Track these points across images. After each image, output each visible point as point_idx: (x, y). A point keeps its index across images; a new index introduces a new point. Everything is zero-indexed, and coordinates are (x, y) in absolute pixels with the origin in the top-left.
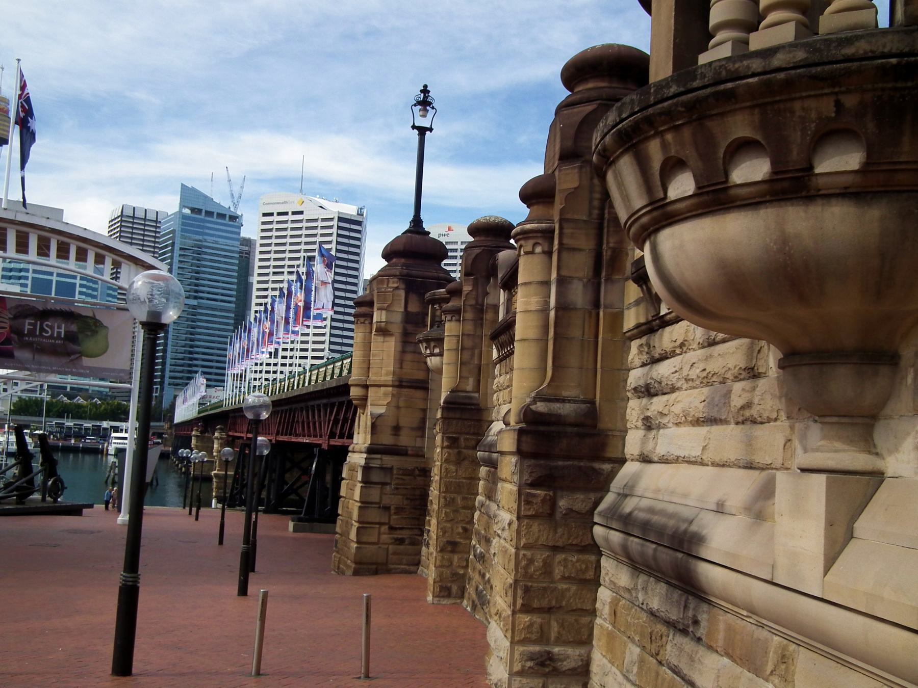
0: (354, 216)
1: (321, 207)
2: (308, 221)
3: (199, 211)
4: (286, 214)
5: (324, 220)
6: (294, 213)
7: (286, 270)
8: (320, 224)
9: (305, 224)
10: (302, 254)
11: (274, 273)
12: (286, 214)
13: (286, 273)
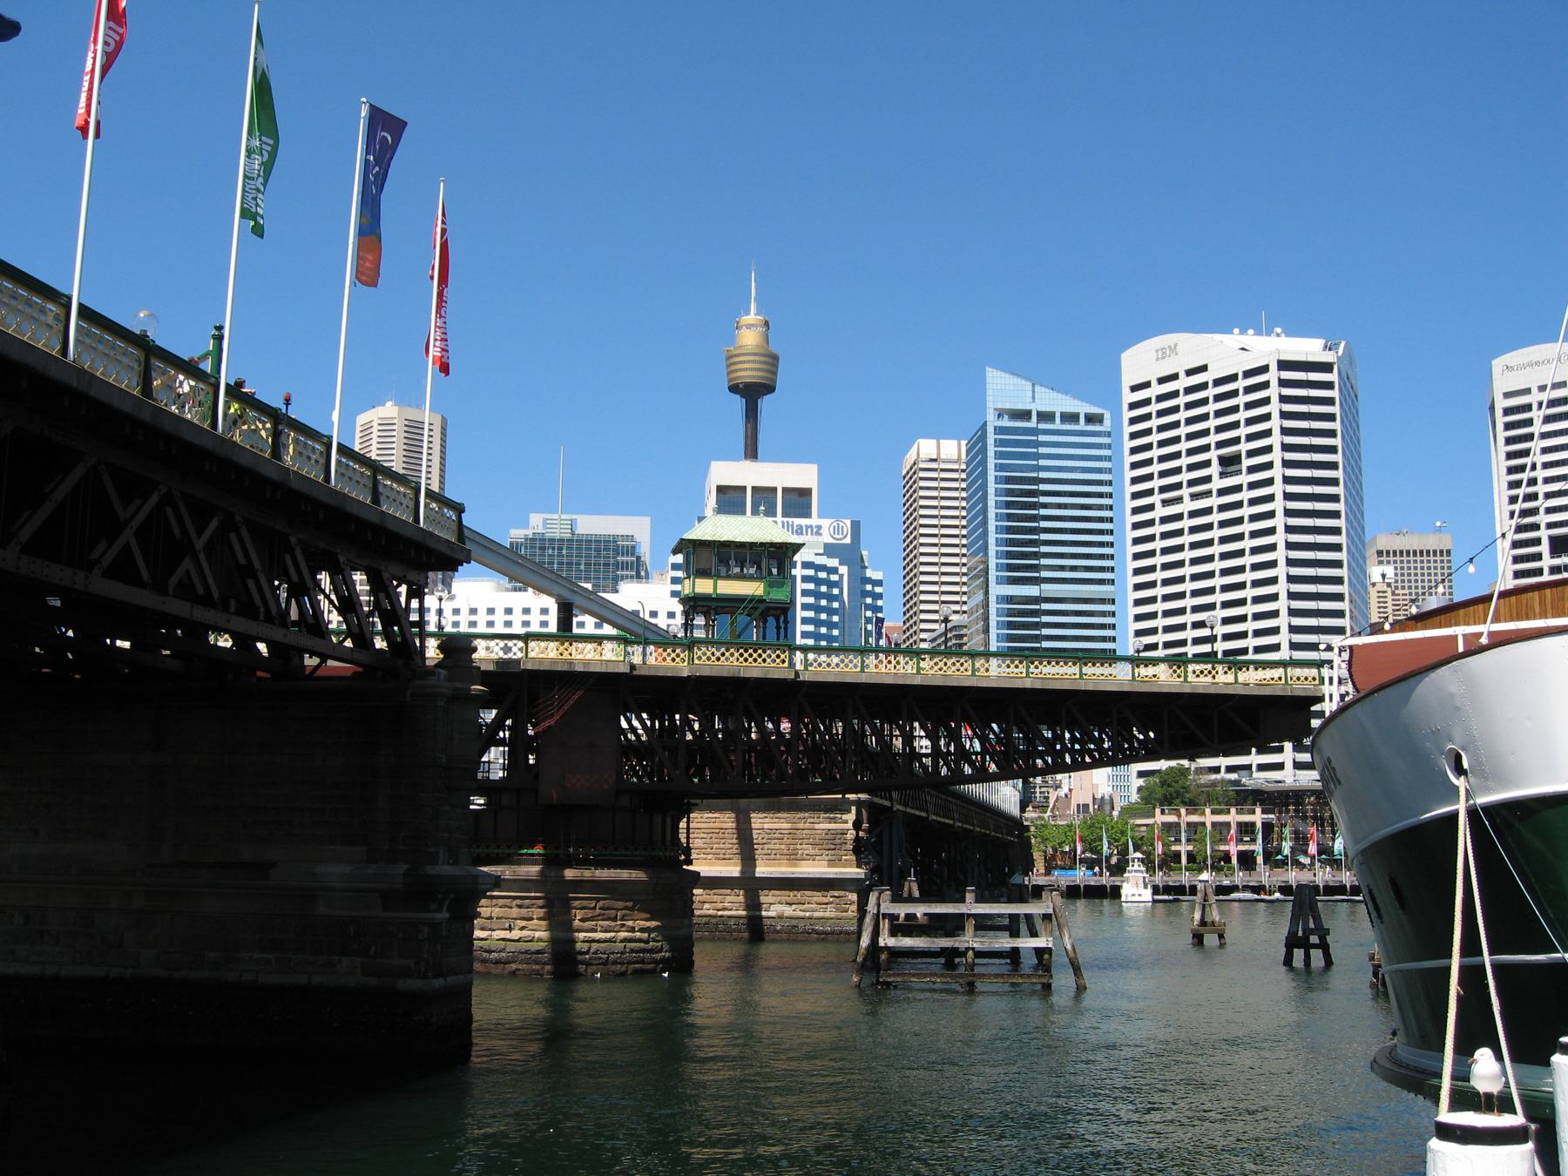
0: (1314, 354)
1: (1243, 349)
2: (1218, 382)
3: (1025, 415)
4: (1175, 377)
5: (1248, 374)
6: (1190, 373)
7: (1185, 492)
8: (1241, 384)
9: (1211, 392)
10: (1213, 455)
11: (1165, 503)
12: (1175, 377)
13: (1186, 498)
